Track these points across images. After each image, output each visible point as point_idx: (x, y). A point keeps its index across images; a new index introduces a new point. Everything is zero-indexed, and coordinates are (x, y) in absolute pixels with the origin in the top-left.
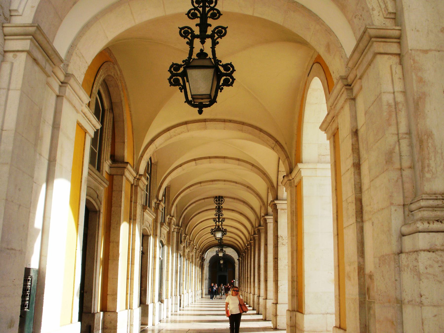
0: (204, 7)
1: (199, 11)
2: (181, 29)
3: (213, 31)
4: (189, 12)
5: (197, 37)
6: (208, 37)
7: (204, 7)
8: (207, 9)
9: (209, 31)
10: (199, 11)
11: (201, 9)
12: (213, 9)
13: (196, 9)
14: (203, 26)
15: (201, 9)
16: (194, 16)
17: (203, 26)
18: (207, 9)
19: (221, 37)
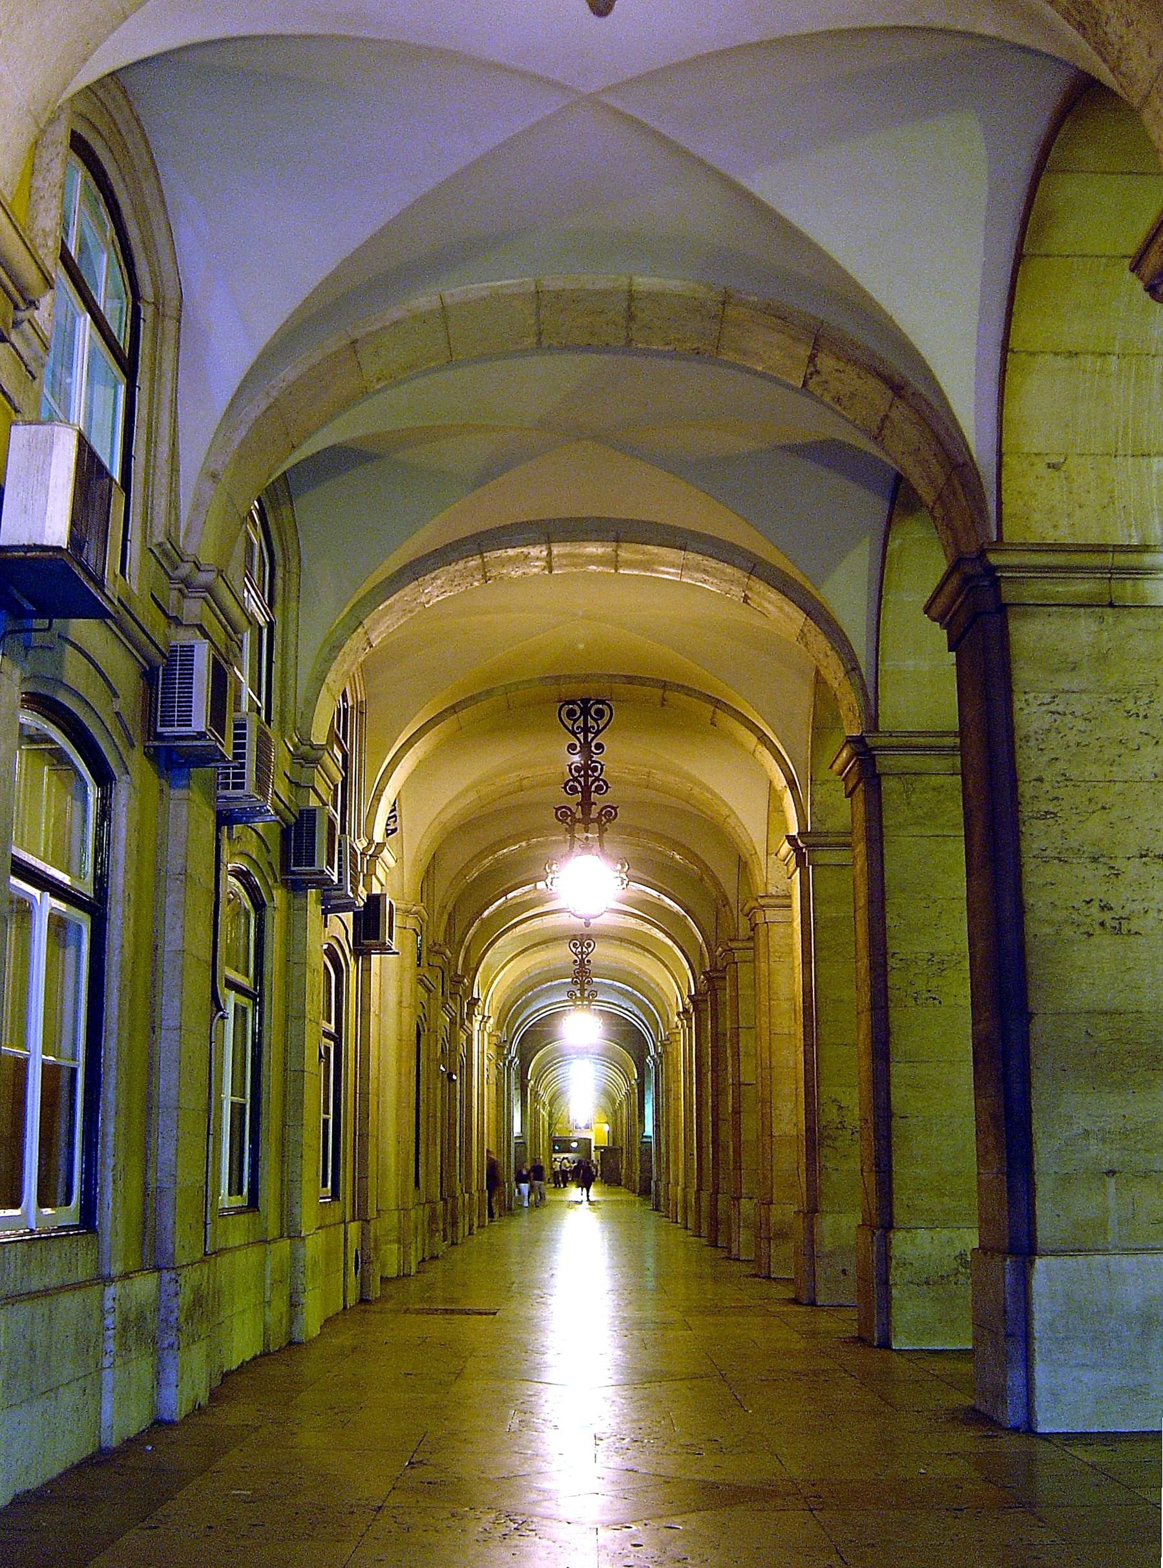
0: (586, 776)
1: (580, 783)
2: (557, 809)
3: (600, 814)
4: (566, 784)
5: (579, 821)
6: (593, 821)
7: (586, 776)
8: (590, 779)
9: (594, 814)
10: (580, 783)
11: (582, 779)
12: (597, 779)
13: (575, 779)
14: (586, 804)
15: (582, 779)
16: (574, 790)
17: (586, 804)
18: (590, 779)
19: (609, 821)
